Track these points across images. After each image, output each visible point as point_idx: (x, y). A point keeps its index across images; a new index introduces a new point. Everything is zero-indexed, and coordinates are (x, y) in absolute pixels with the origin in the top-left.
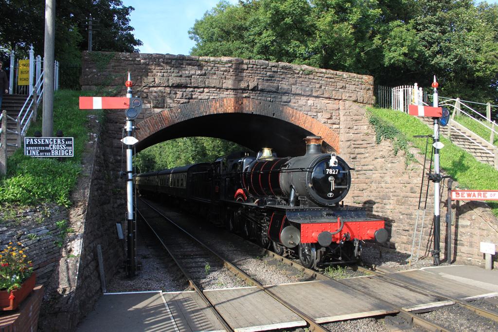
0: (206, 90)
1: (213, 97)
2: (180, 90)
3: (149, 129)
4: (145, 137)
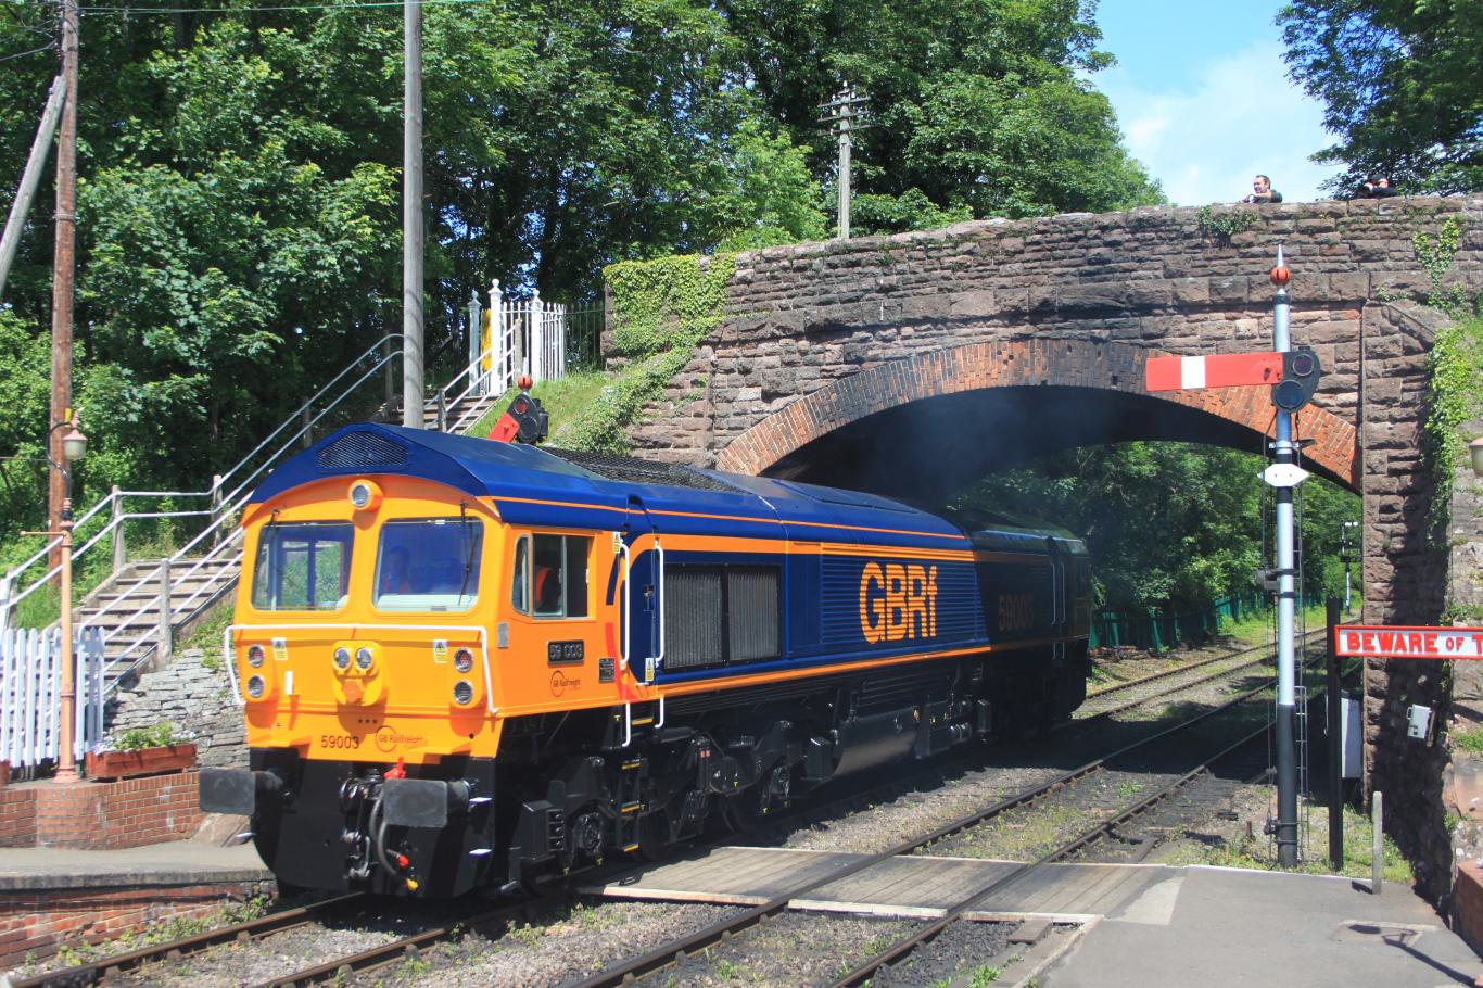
0: (908, 330)
1: (922, 349)
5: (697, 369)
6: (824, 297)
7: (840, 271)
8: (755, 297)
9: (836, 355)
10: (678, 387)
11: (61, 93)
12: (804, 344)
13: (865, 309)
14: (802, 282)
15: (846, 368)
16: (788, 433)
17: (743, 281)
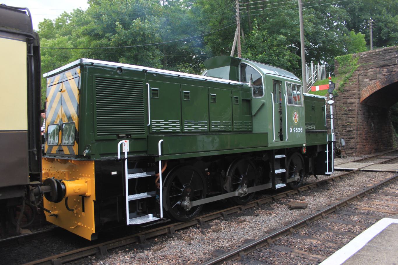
2: (386, 67)
3: (369, 92)
4: (367, 96)
5: (355, 76)
6: (383, 60)
7: (386, 54)
8: (367, 61)
9: (386, 71)
10: (351, 79)
11: (238, 31)
12: (378, 69)
13: (393, 61)
14: (378, 57)
15: (388, 73)
16: (375, 87)
17: (365, 58)
